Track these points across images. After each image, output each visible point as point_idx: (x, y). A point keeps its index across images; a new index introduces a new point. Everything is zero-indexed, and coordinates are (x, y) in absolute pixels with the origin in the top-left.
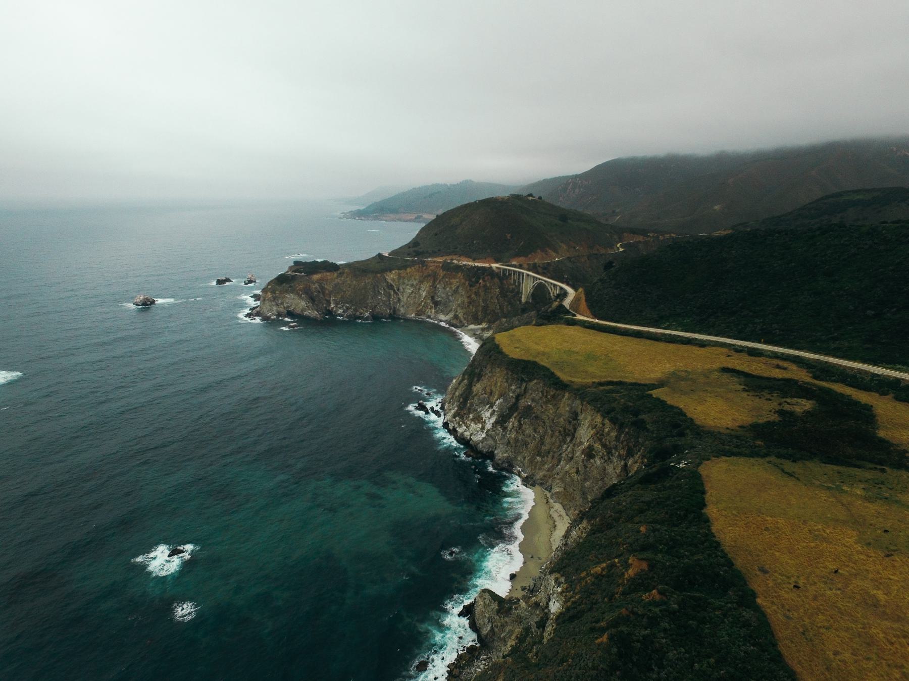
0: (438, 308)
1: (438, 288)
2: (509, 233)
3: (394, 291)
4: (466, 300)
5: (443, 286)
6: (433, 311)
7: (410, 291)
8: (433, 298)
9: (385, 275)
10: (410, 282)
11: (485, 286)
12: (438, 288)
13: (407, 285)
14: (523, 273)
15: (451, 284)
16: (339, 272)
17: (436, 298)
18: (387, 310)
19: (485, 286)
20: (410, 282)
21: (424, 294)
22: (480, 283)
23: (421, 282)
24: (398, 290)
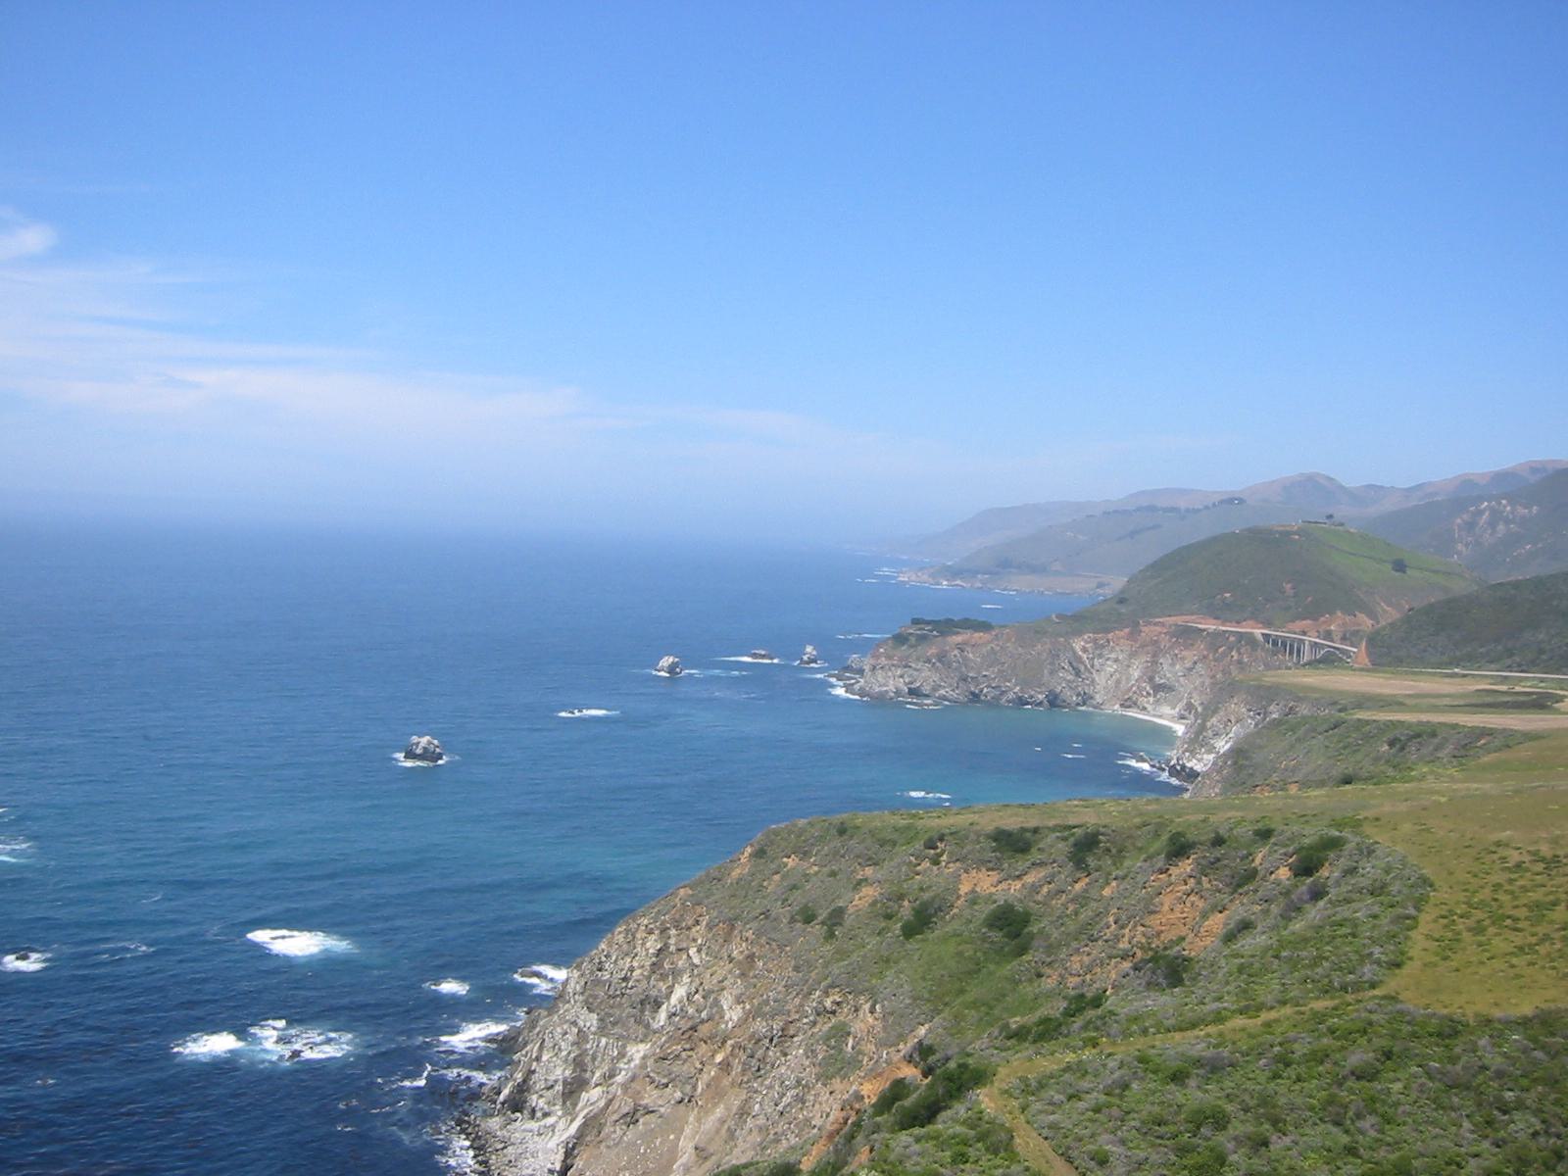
0: (1158, 697)
1: (1161, 664)
2: (1289, 582)
3: (1086, 666)
4: (1208, 681)
5: (1170, 661)
6: (1151, 699)
7: (1113, 670)
8: (1151, 679)
9: (1071, 641)
10: (1113, 656)
11: (1240, 662)
12: (1161, 664)
13: (1108, 659)
14: (1303, 641)
15: (1183, 659)
16: (994, 633)
17: (1157, 679)
18: (1072, 697)
19: (1240, 662)
20: (1113, 656)
21: (1136, 674)
22: (1232, 657)
23: (1133, 655)
24: (1092, 666)
